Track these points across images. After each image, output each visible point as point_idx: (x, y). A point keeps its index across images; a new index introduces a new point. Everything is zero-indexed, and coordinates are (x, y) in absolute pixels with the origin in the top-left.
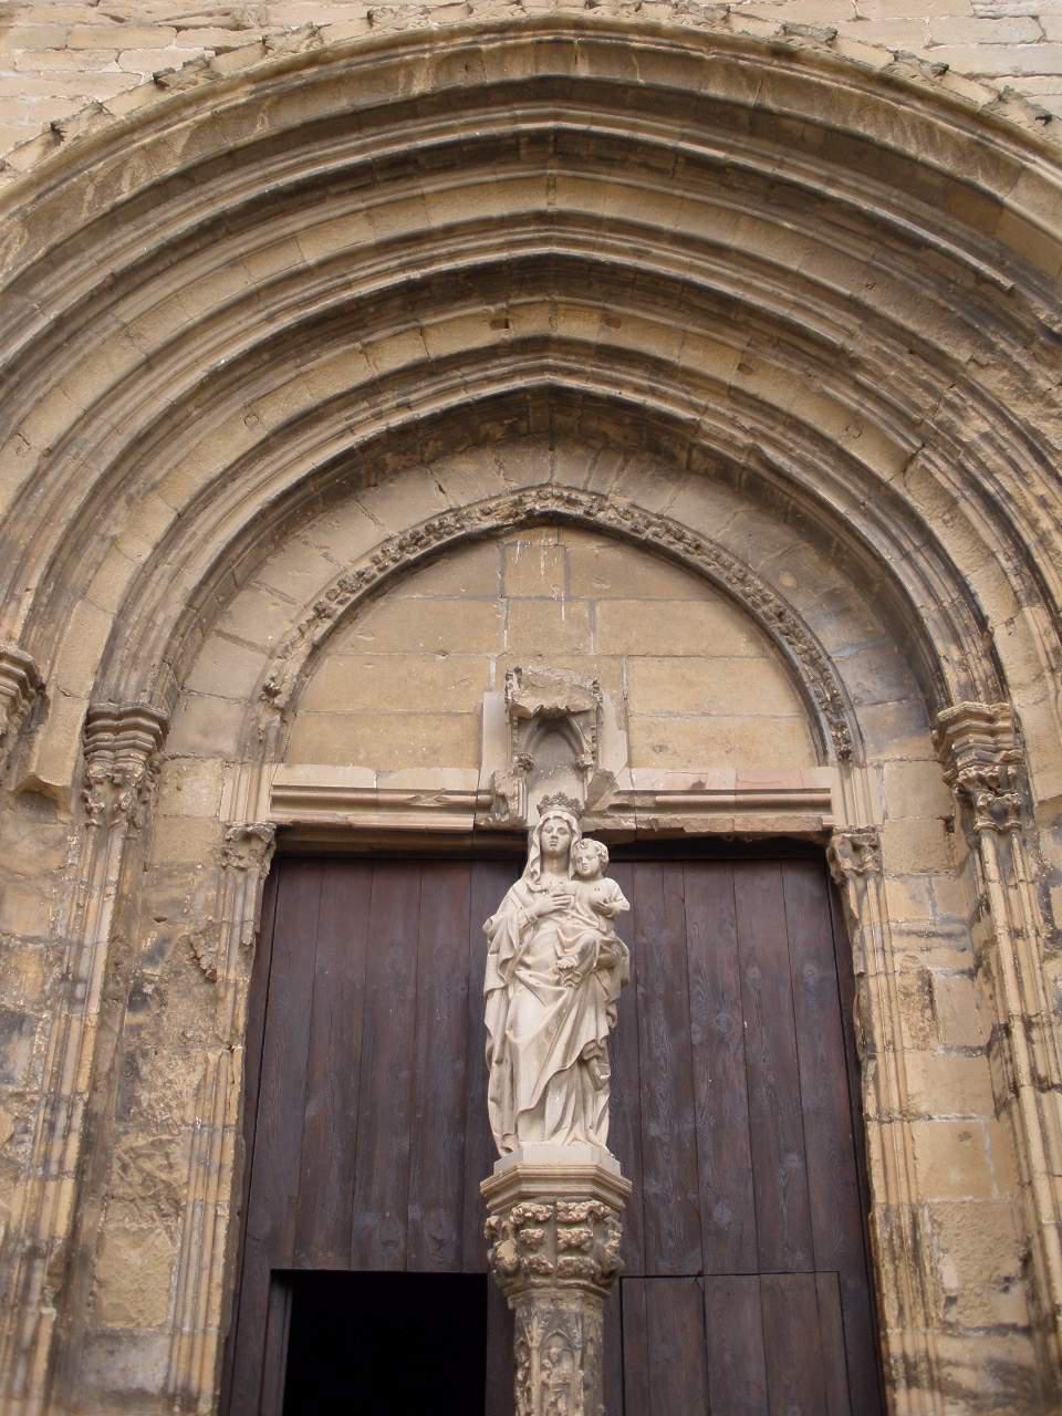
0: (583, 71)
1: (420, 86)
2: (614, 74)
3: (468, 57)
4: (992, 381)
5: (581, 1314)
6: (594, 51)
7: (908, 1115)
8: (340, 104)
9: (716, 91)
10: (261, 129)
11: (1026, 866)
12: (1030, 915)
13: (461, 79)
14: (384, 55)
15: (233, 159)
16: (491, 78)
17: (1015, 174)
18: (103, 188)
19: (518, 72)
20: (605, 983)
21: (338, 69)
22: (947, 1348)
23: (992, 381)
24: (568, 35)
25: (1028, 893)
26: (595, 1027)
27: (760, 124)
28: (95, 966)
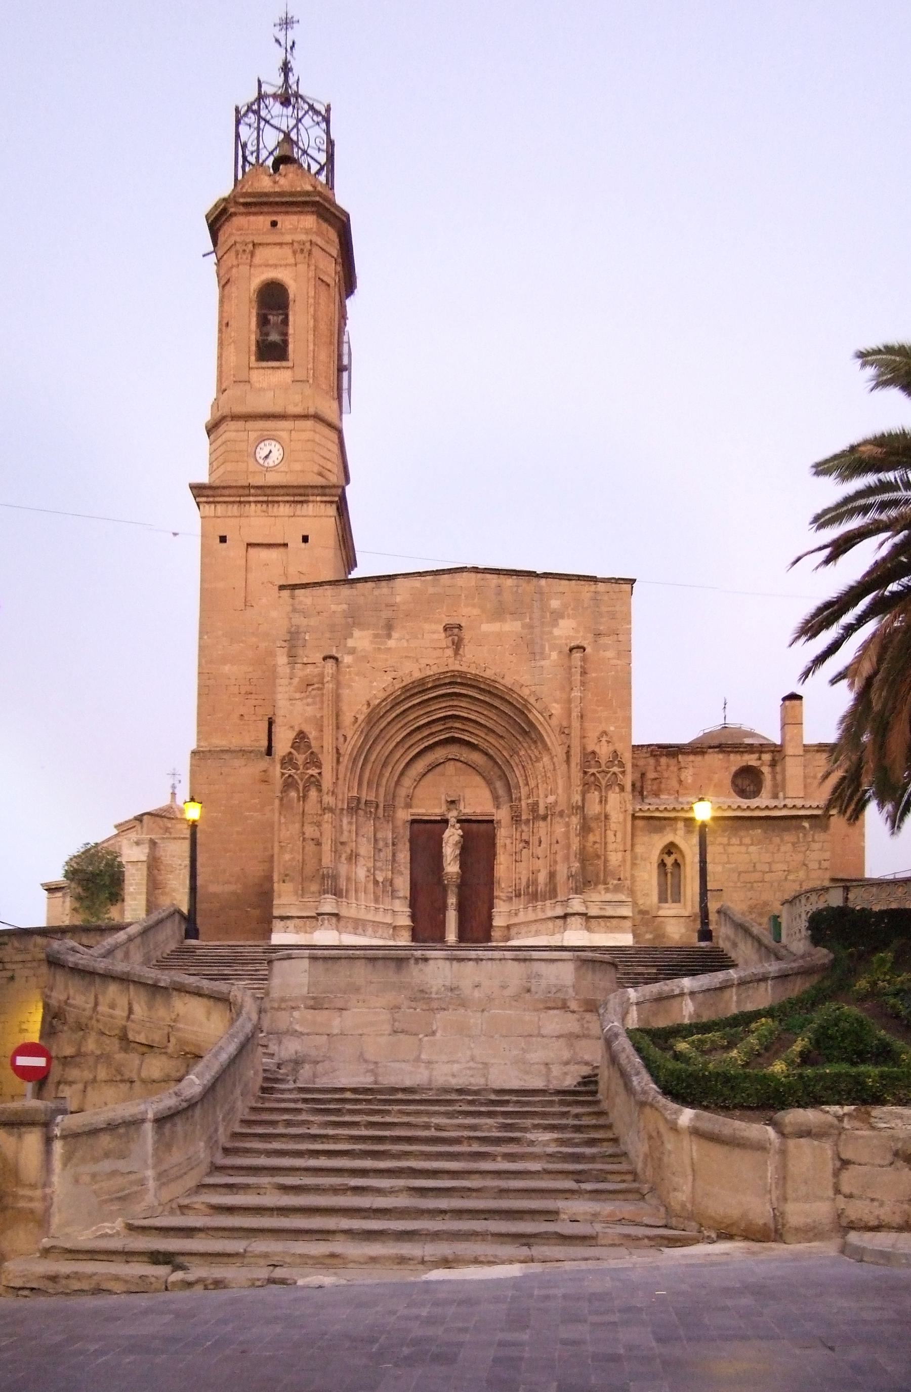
0: (459, 680)
1: (429, 686)
2: (464, 681)
3: (439, 679)
4: (525, 745)
5: (455, 890)
6: (460, 677)
7: (500, 864)
8: (416, 690)
9: (482, 686)
10: (403, 697)
11: (519, 829)
12: (518, 837)
13: (437, 683)
14: (422, 681)
15: (398, 704)
16: (442, 682)
17: (530, 711)
18: (379, 712)
19: (447, 681)
20: (460, 845)
21: (416, 684)
22: (501, 894)
23: (525, 745)
24: (456, 673)
25: (518, 834)
26: (458, 852)
27: (490, 692)
28: (390, 842)
